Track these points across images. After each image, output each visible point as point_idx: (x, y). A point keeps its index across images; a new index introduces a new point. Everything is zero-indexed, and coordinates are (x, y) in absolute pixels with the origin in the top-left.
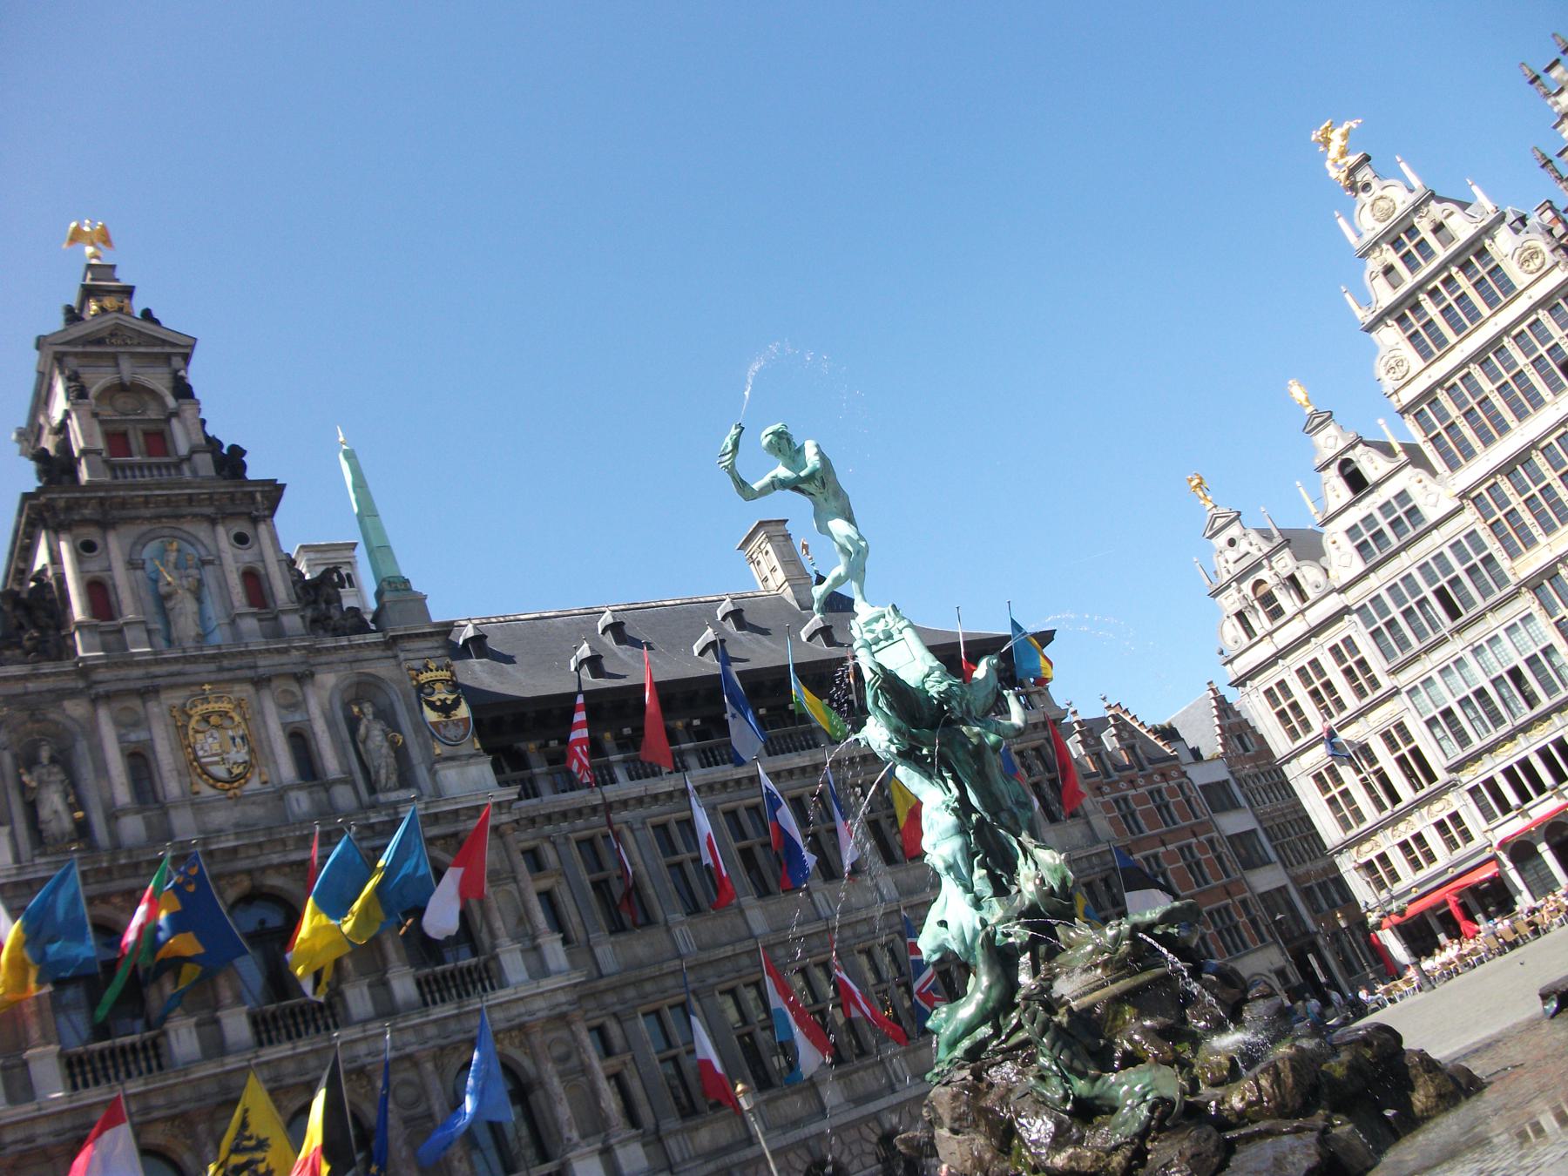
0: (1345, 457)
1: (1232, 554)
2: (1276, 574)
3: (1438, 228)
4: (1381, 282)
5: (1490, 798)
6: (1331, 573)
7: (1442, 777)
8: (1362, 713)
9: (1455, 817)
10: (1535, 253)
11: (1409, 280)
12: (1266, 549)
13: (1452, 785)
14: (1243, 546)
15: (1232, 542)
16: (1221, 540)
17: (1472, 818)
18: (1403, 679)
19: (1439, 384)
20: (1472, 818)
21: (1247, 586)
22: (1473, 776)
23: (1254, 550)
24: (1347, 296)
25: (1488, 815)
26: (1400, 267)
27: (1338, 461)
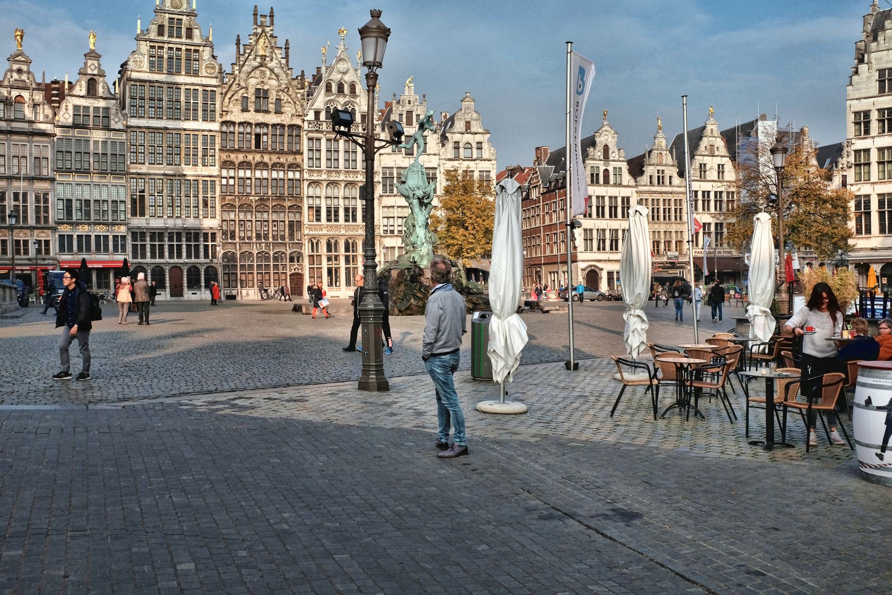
0: (94, 77)
1: (15, 76)
2: (33, 100)
3: (189, 31)
4: (154, 28)
5: (65, 243)
6: (57, 118)
7: (51, 223)
8: (31, 179)
9: (47, 243)
10: (213, 68)
11: (166, 38)
12: (34, 86)
13: (54, 229)
14: (24, 77)
15: (19, 71)
16: (15, 67)
17: (54, 248)
18: (58, 178)
19: (150, 81)
20: (54, 248)
21: (15, 93)
22: (65, 230)
23: (27, 81)
24: (139, 21)
25: (62, 249)
26: (166, 29)
27: (91, 77)
